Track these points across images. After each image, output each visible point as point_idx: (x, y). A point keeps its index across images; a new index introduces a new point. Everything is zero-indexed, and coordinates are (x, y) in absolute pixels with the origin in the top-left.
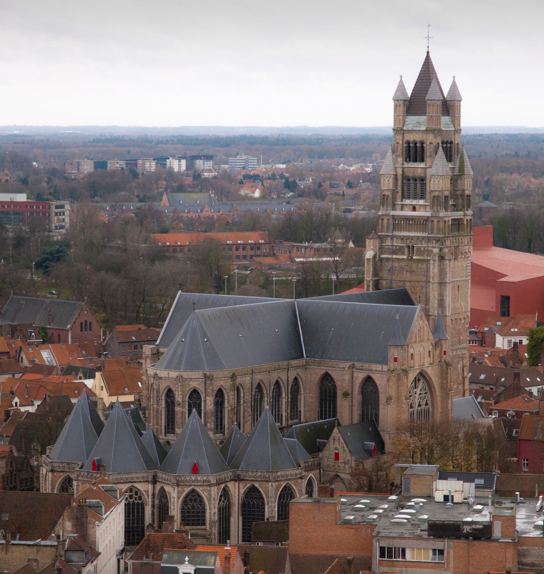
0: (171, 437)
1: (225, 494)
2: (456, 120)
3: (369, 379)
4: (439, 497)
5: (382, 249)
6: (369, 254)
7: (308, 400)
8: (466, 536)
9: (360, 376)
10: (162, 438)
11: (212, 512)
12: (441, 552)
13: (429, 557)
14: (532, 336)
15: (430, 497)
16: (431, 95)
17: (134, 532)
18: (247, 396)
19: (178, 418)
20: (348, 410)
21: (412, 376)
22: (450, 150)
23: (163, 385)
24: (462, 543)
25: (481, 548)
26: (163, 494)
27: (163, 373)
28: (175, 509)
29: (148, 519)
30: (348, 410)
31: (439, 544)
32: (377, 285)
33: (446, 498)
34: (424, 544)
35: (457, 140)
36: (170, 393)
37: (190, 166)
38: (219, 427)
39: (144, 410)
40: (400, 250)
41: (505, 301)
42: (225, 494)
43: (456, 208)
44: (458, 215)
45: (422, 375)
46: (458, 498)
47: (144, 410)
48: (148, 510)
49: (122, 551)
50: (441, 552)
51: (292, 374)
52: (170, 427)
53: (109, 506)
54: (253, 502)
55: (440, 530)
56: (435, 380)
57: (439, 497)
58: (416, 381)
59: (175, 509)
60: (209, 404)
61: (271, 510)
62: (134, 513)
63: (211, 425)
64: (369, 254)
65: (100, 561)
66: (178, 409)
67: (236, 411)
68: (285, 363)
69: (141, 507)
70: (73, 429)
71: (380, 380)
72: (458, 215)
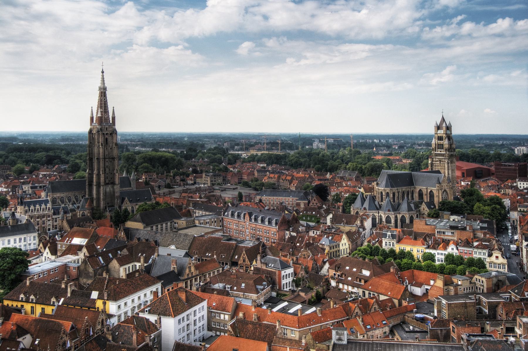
0: (382, 203)
1: (396, 217)
2: (451, 131)
3: (431, 191)
4: (451, 220)
5: (433, 161)
6: (430, 162)
7: (416, 195)
8: (460, 229)
9: (429, 191)
10: (380, 203)
11: (393, 221)
12: (453, 233)
13: (450, 234)
14: (471, 182)
15: (449, 219)
16: (444, 125)
17: (374, 225)
18: (401, 194)
19: (384, 199)
20: (426, 199)
21: (443, 191)
22: (449, 137)
23: (380, 191)
24: (459, 231)
25: (464, 233)
26: (381, 216)
27: (380, 188)
28: (384, 219)
29: (377, 222)
30: (426, 199)
31: (453, 231)
32: (432, 169)
33: (453, 220)
34: (448, 231)
35: (451, 136)
36: (382, 193)
37: (380, 141)
38: (394, 201)
39: (375, 196)
40: (438, 161)
41: (463, 173)
42: (396, 217)
43: (451, 151)
44: (452, 153)
45: (445, 190)
46: (456, 220)
47: (375, 196)
48: (377, 219)
49: (371, 229)
50: (453, 233)
51: (412, 189)
52: (382, 201)
53: (368, 218)
54: (403, 219)
55: (452, 228)
56: (448, 192)
57: (451, 220)
58: (443, 192)
59: (384, 219)
60: (391, 196)
61: (408, 221)
62: (374, 220)
63: (392, 201)
64: (430, 162)
65: (367, 231)
66: (384, 197)
67: (398, 198)
68: (410, 187)
69: (376, 219)
70: (358, 201)
71: (435, 192)
72: (452, 153)
